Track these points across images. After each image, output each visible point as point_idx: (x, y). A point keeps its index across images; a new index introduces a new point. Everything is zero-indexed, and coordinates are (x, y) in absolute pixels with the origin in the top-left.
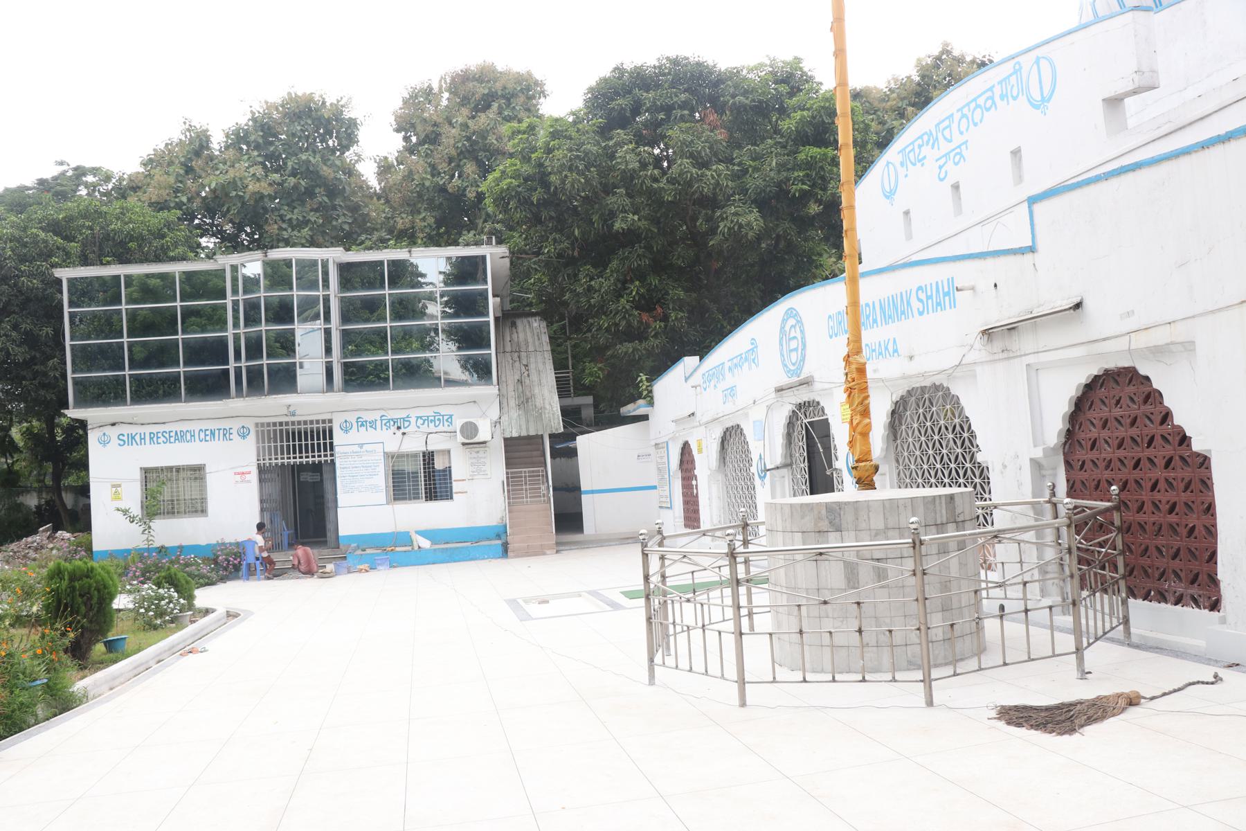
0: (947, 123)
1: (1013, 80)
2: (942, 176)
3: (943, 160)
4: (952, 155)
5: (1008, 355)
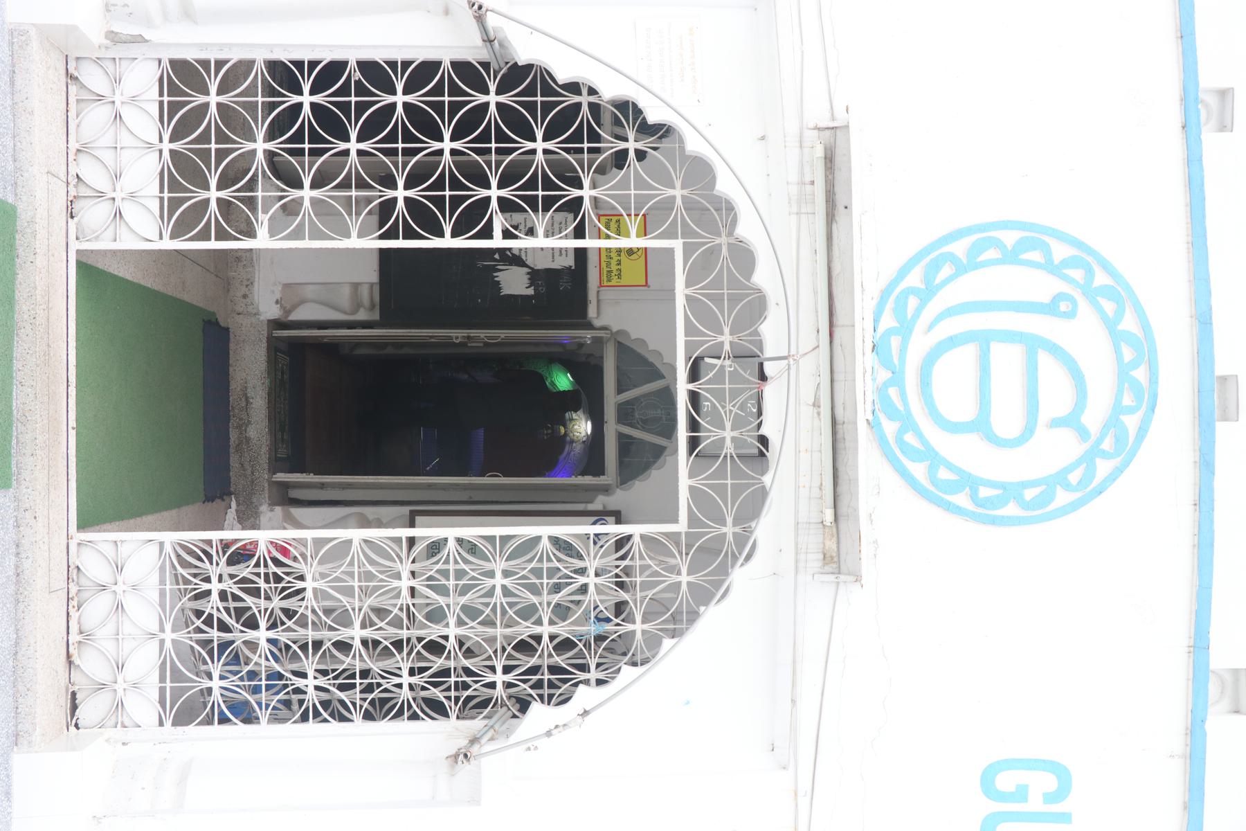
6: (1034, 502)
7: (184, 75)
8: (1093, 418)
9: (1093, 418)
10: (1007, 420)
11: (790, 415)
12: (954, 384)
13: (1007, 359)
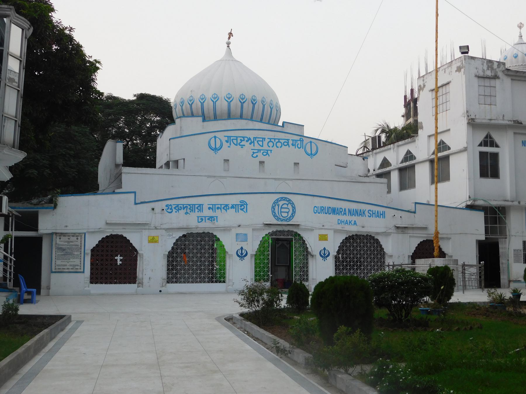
0: (261, 140)
1: (299, 142)
3: (257, 151)
4: (262, 151)
5: (403, 233)
6: (294, 208)
7: (256, 281)
8: (287, 203)
9: (287, 203)
10: (287, 210)
11: (286, 229)
12: (285, 215)
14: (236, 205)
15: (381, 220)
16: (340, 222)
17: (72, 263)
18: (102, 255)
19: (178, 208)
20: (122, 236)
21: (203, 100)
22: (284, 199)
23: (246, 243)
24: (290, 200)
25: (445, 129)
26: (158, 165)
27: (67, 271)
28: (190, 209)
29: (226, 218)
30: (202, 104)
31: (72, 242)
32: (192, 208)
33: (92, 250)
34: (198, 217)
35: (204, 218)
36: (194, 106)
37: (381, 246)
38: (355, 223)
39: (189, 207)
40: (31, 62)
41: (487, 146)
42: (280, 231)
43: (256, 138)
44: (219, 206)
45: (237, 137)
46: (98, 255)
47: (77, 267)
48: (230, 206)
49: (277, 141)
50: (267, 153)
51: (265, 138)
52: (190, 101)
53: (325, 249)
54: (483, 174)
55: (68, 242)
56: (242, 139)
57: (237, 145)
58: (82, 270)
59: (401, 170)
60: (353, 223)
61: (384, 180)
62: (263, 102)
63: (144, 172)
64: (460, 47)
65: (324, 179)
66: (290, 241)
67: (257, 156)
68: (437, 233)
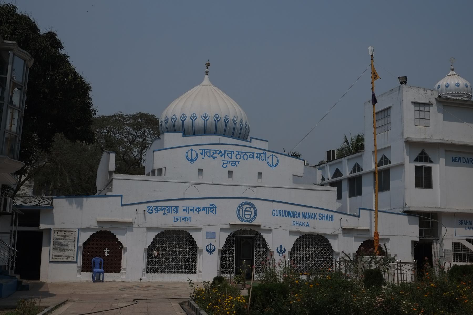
0: (231, 152)
2: (225, 166)
6: (256, 211)
10: (250, 213)
11: (248, 229)
12: (248, 217)
13: (246, 213)
14: (206, 208)
15: (329, 223)
16: (295, 224)
17: (67, 254)
18: (93, 248)
19: (158, 209)
20: (110, 232)
21: (184, 118)
22: (247, 204)
23: (214, 240)
24: (252, 204)
25: (387, 146)
26: (146, 172)
27: (62, 260)
28: (167, 210)
29: (197, 219)
30: (183, 122)
31: (67, 236)
32: (169, 210)
33: (84, 244)
34: (174, 217)
35: (179, 218)
36: (176, 123)
37: (330, 244)
38: (308, 225)
39: (167, 209)
40: (33, 89)
41: (422, 161)
42: (244, 230)
43: (226, 151)
44: (193, 208)
45: (210, 150)
46: (89, 248)
47: (71, 258)
48: (201, 208)
49: (244, 154)
50: (235, 164)
51: (234, 152)
52: (173, 119)
53: (281, 246)
54: (419, 185)
55: (64, 236)
56: (215, 152)
57: (210, 157)
58: (75, 260)
59: (350, 180)
60: (306, 224)
61: (335, 189)
62: (234, 121)
63: (131, 178)
64: (399, 78)
65: (283, 187)
66: (252, 238)
67: (227, 166)
68: (377, 234)
